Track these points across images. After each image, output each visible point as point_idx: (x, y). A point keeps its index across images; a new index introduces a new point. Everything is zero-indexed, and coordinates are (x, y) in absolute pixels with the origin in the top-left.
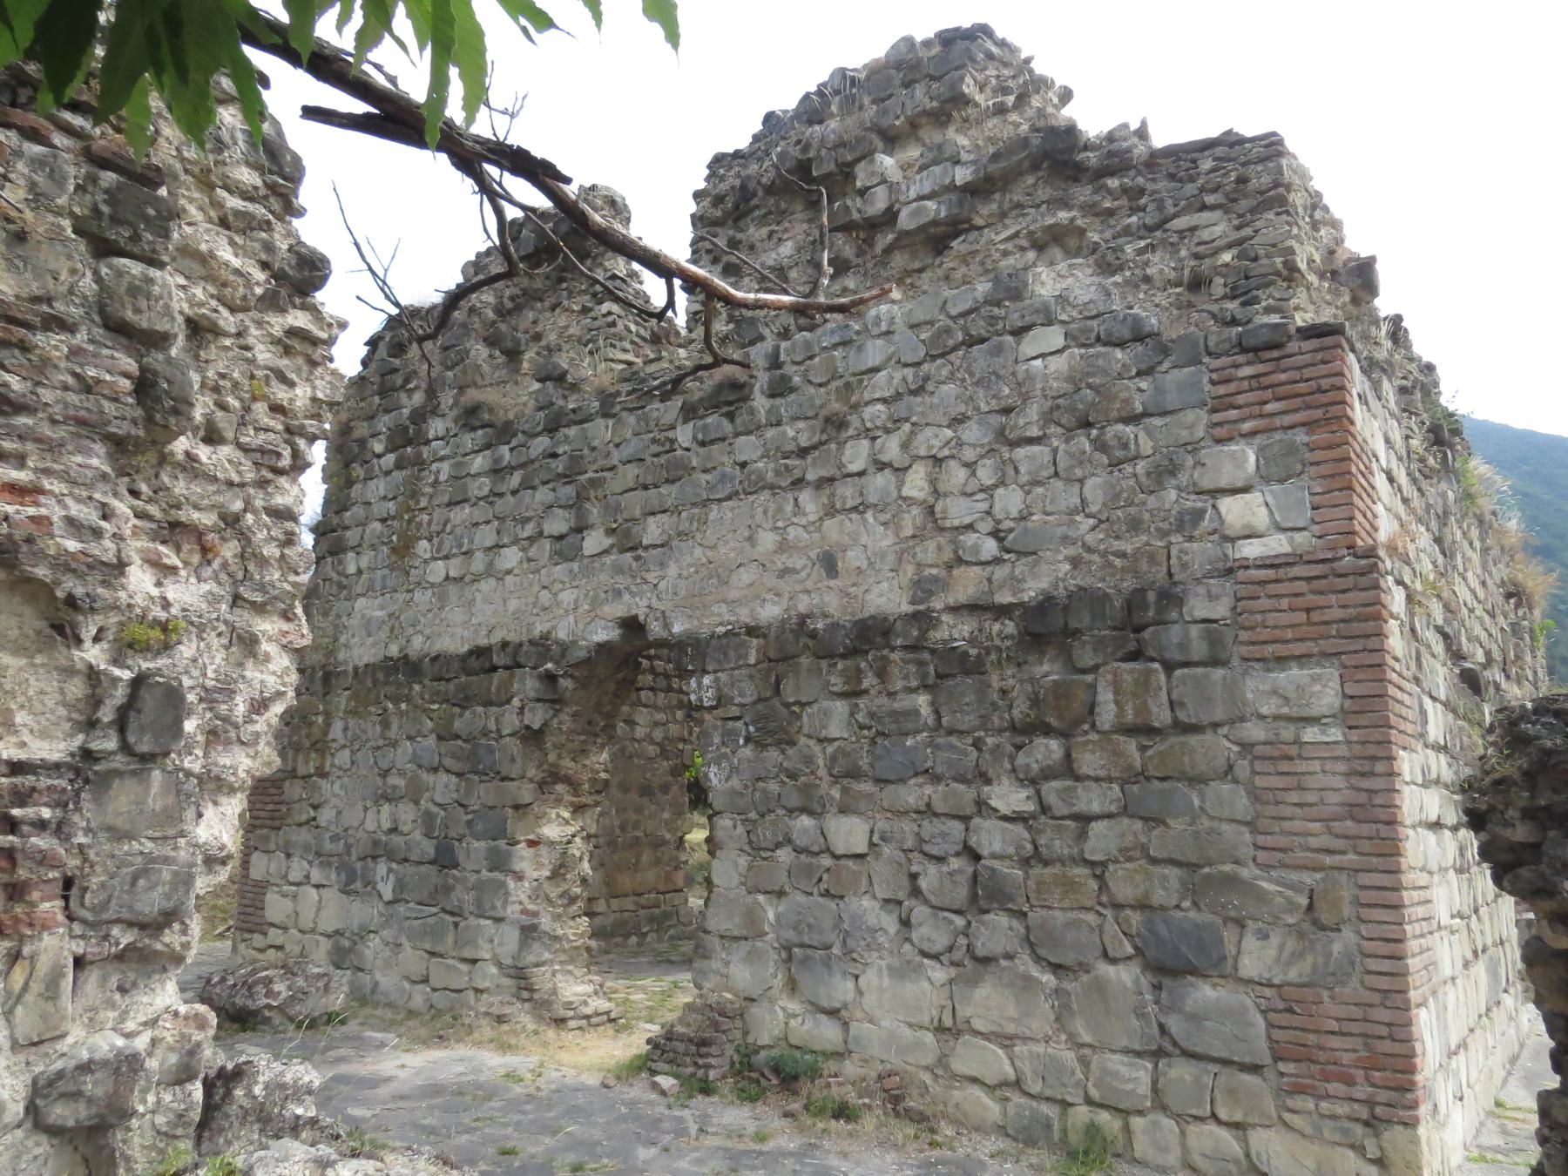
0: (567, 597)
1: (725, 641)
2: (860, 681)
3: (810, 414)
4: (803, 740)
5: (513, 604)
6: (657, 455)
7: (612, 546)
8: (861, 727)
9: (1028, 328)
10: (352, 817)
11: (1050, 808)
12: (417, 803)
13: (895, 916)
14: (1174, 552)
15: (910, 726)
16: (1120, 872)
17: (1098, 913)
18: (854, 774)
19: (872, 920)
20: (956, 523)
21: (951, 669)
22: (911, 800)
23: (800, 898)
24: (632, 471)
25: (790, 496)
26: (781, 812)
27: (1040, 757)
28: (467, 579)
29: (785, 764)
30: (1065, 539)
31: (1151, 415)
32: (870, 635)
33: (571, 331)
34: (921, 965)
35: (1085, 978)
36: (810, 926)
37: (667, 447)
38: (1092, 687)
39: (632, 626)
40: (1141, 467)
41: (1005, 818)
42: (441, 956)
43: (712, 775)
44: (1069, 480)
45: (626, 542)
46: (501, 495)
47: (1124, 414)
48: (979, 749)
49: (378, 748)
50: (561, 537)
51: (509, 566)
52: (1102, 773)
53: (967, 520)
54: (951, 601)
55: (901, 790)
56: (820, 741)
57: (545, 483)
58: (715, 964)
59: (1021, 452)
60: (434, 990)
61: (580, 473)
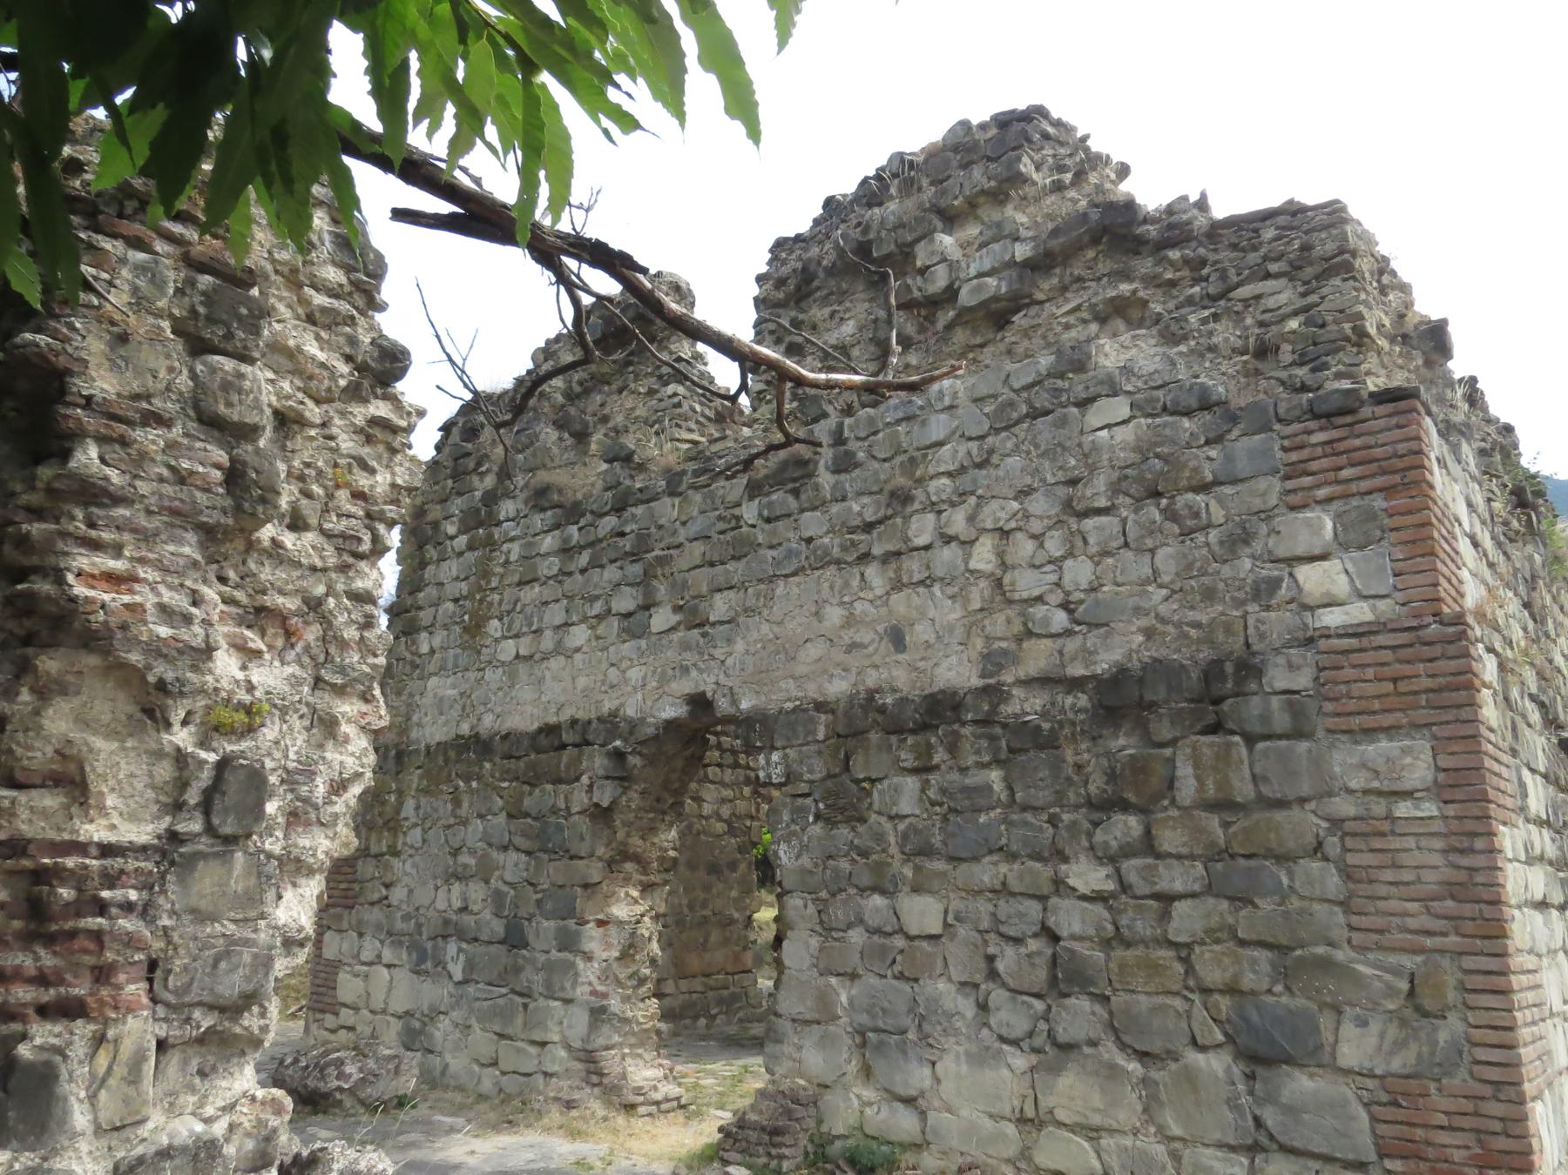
0: (635, 674)
1: (793, 717)
2: (931, 758)
3: (875, 489)
4: (873, 817)
5: (582, 681)
6: (722, 532)
7: (679, 623)
8: (933, 804)
9: (1092, 400)
10: (423, 897)
11: (1130, 887)
12: (487, 882)
13: (972, 999)
14: (1251, 622)
15: (982, 802)
16: (1207, 955)
17: (1185, 997)
18: (926, 851)
19: (948, 1004)
20: (1025, 595)
22: (986, 879)
23: (873, 980)
24: (698, 549)
25: (856, 570)
26: (852, 891)
27: (1119, 835)
28: (537, 657)
29: (856, 842)
30: (1138, 611)
31: (1222, 484)
32: (940, 710)
33: (638, 413)
34: (1000, 1051)
35: (1173, 1066)
36: (884, 1010)
37: (733, 523)
38: (1171, 762)
39: (700, 703)
40: (1213, 536)
41: (1084, 898)
42: (511, 1039)
43: (781, 853)
44: (1140, 551)
45: (694, 619)
46: (570, 574)
47: (1194, 483)
48: (1055, 826)
49: (449, 827)
50: (629, 615)
51: (578, 643)
52: (1184, 850)
53: (1036, 593)
54: (1022, 674)
55: (976, 868)
56: (891, 818)
58: (787, 1049)
59: (1089, 523)
60: (504, 1073)
61: (647, 552)
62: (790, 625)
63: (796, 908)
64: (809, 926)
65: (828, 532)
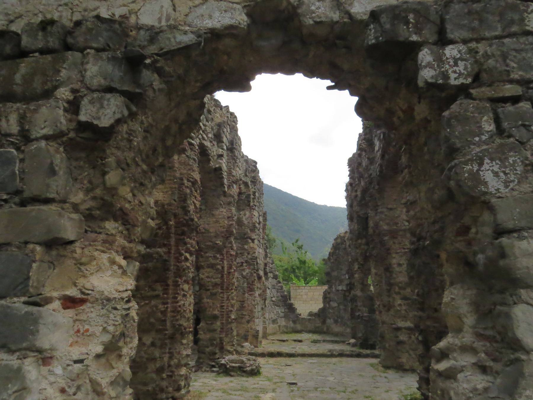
43: (488, 176)
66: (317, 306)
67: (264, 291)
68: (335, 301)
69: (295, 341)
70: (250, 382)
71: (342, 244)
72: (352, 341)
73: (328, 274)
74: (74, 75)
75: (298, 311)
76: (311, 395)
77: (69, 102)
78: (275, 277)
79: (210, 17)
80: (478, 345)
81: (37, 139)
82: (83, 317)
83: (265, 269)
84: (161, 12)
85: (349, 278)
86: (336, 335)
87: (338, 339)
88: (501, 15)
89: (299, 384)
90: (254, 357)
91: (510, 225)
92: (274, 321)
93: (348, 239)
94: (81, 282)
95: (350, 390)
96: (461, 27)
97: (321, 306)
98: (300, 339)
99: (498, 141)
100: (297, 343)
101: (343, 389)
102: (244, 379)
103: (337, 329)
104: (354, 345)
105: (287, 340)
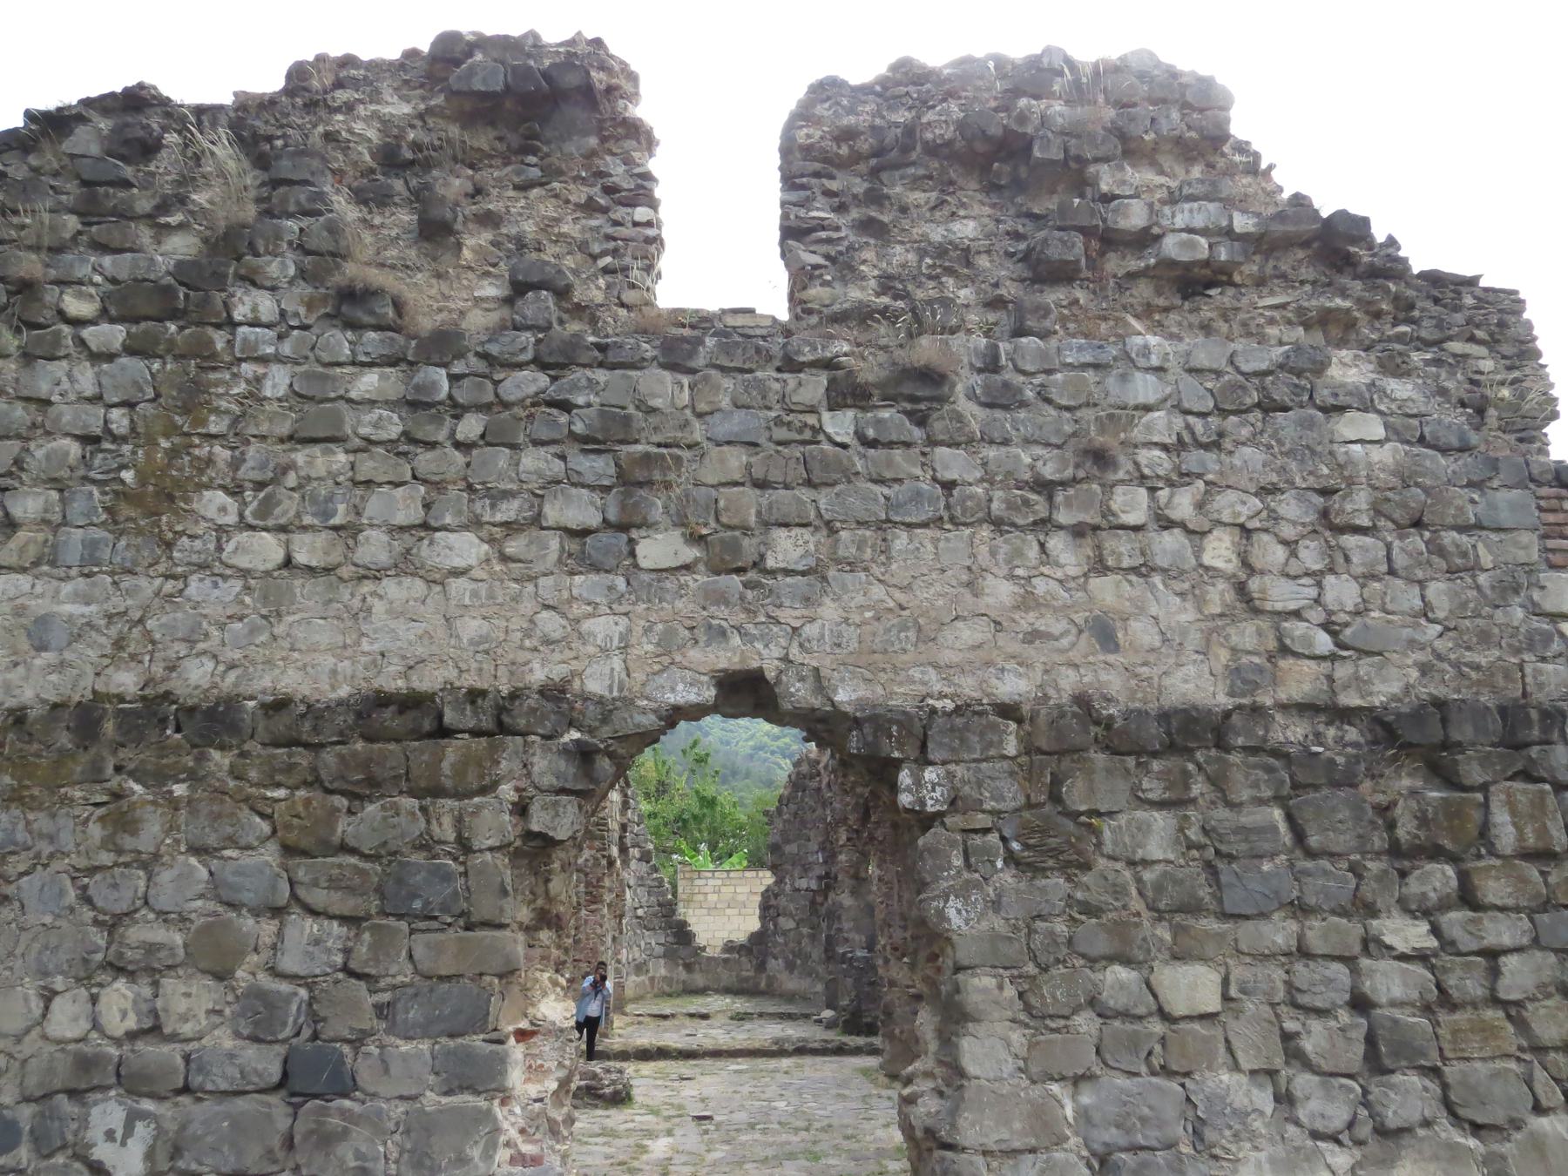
0: (603, 627)
1: (959, 721)
2: (1187, 788)
3: (1054, 440)
4: (1102, 863)
5: (471, 627)
7: (697, 561)
8: (1191, 846)
9: (1341, 409)
11: (1453, 943)
12: (222, 975)
13: (1270, 1090)
14: (1528, 670)
15: (1267, 846)
16: (1542, 1011)
17: (1518, 1059)
18: (1193, 908)
19: (1239, 1100)
20: (1279, 606)
21: (1300, 778)
22: (1280, 940)
23: (1121, 1081)
24: (736, 461)
26: (1079, 962)
27: (1438, 885)
28: (345, 572)
29: (1079, 895)
30: (1412, 644)
31: (1483, 528)
32: (1189, 733)
33: (565, 228)
34: (1317, 1150)
35: (1518, 1136)
36: (1144, 1120)
37: (807, 435)
38: (1486, 805)
40: (1483, 579)
41: (1403, 957)
43: (951, 913)
44: (1410, 581)
47: (1460, 521)
48: (1359, 876)
49: (93, 870)
50: (583, 533)
51: (459, 563)
52: (1510, 902)
53: (1292, 606)
54: (1283, 696)
55: (1265, 927)
56: (1131, 863)
57: (538, 443)
59: (1350, 541)
61: (622, 442)
62: (923, 593)
63: (985, 991)
64: (1009, 1014)
65: (982, 480)
66: (745, 924)
67: (620, 896)
68: (791, 916)
69: (692, 1016)
70: (616, 1118)
71: (812, 778)
72: (828, 1014)
73: (775, 848)
74: (516, 766)
75: (701, 940)
76: (743, 1138)
77: (513, 804)
78: (645, 857)
79: (673, 690)
80: (937, 1071)
81: (481, 851)
82: (535, 1051)
83: (621, 838)
84: (612, 677)
85: (825, 862)
86: (790, 997)
87: (792, 1009)
88: (982, 734)
89: (717, 1118)
90: (618, 1065)
91: (966, 963)
92: (640, 968)
93: (826, 767)
94: (531, 1011)
95: (817, 1125)
96: (941, 744)
97: (754, 924)
98: (704, 1011)
99: (966, 875)
100: (697, 1021)
101: (801, 1124)
102: (599, 1112)
103: (791, 983)
104: (830, 1025)
105: (673, 1015)
